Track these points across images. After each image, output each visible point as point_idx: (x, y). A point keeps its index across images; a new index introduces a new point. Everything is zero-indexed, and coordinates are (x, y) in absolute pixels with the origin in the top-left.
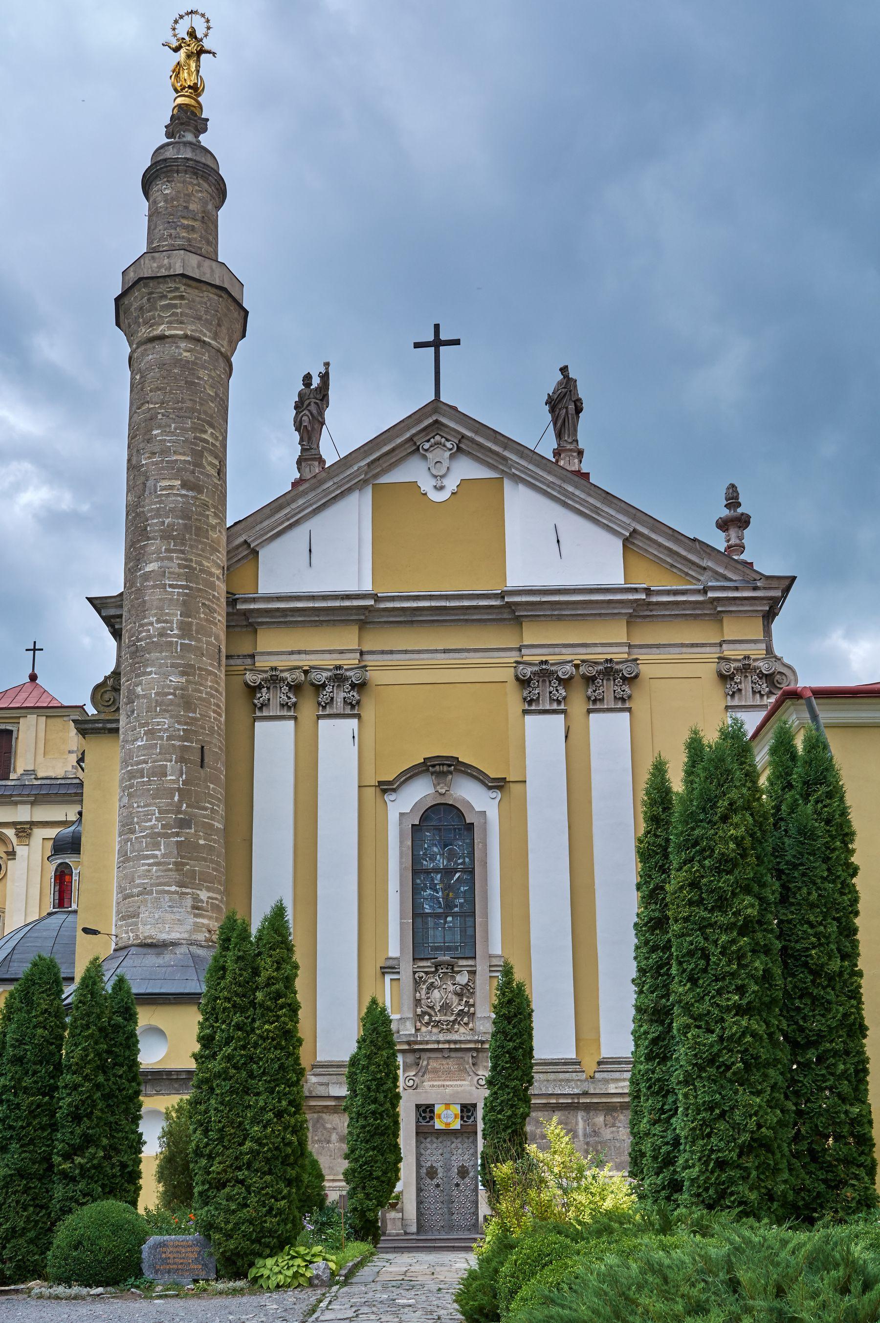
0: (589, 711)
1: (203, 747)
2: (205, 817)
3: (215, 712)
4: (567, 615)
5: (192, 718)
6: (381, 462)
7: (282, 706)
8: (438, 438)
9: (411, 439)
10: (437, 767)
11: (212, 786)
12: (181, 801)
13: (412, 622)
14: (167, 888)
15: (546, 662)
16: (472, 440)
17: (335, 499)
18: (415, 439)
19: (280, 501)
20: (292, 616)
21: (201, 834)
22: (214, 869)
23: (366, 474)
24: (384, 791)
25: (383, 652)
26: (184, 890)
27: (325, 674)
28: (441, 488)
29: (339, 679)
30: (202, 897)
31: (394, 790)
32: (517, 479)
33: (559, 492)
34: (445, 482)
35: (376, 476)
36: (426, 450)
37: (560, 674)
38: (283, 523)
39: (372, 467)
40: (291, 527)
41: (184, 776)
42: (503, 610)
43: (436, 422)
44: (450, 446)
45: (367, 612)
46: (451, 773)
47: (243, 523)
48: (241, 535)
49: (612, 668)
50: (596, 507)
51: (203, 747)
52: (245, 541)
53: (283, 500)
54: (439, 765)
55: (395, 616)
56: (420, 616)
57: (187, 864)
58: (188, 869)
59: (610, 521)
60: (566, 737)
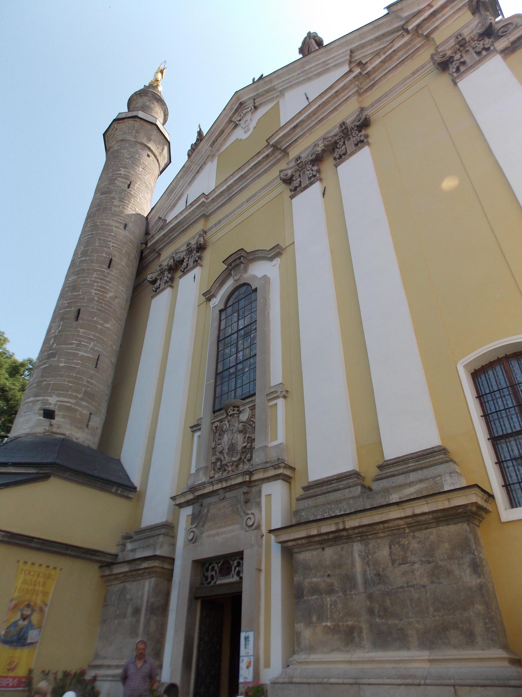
0: (336, 166)
1: (79, 311)
2: (69, 349)
3: (96, 290)
4: (314, 126)
5: (76, 295)
6: (218, 141)
7: (165, 283)
8: (244, 112)
9: (230, 121)
10: (233, 264)
11: (82, 330)
12: (53, 344)
13: (230, 199)
14: (28, 400)
15: (300, 158)
16: (258, 96)
17: (198, 172)
18: (233, 120)
19: (170, 188)
20: (173, 235)
21: (63, 360)
22: (68, 382)
23: (212, 151)
24: (209, 300)
25: (216, 225)
26: (38, 398)
27: (184, 253)
28: (248, 130)
29: (190, 251)
30: (51, 401)
31: (214, 296)
32: (282, 93)
33: (304, 76)
34: (250, 127)
35: (218, 150)
36: (240, 121)
37: (310, 158)
38: (174, 199)
39: (214, 146)
40: (179, 198)
41: (60, 328)
42: (276, 154)
43: (241, 104)
44: (250, 109)
45: (203, 208)
46: (242, 263)
47: (155, 209)
48: (156, 216)
49: (346, 128)
50: (324, 62)
51: (79, 311)
52: (160, 218)
53: (171, 186)
54: (234, 261)
55: (221, 201)
56: (233, 191)
57: (45, 381)
58: (46, 384)
59: (336, 61)
60: (324, 194)
